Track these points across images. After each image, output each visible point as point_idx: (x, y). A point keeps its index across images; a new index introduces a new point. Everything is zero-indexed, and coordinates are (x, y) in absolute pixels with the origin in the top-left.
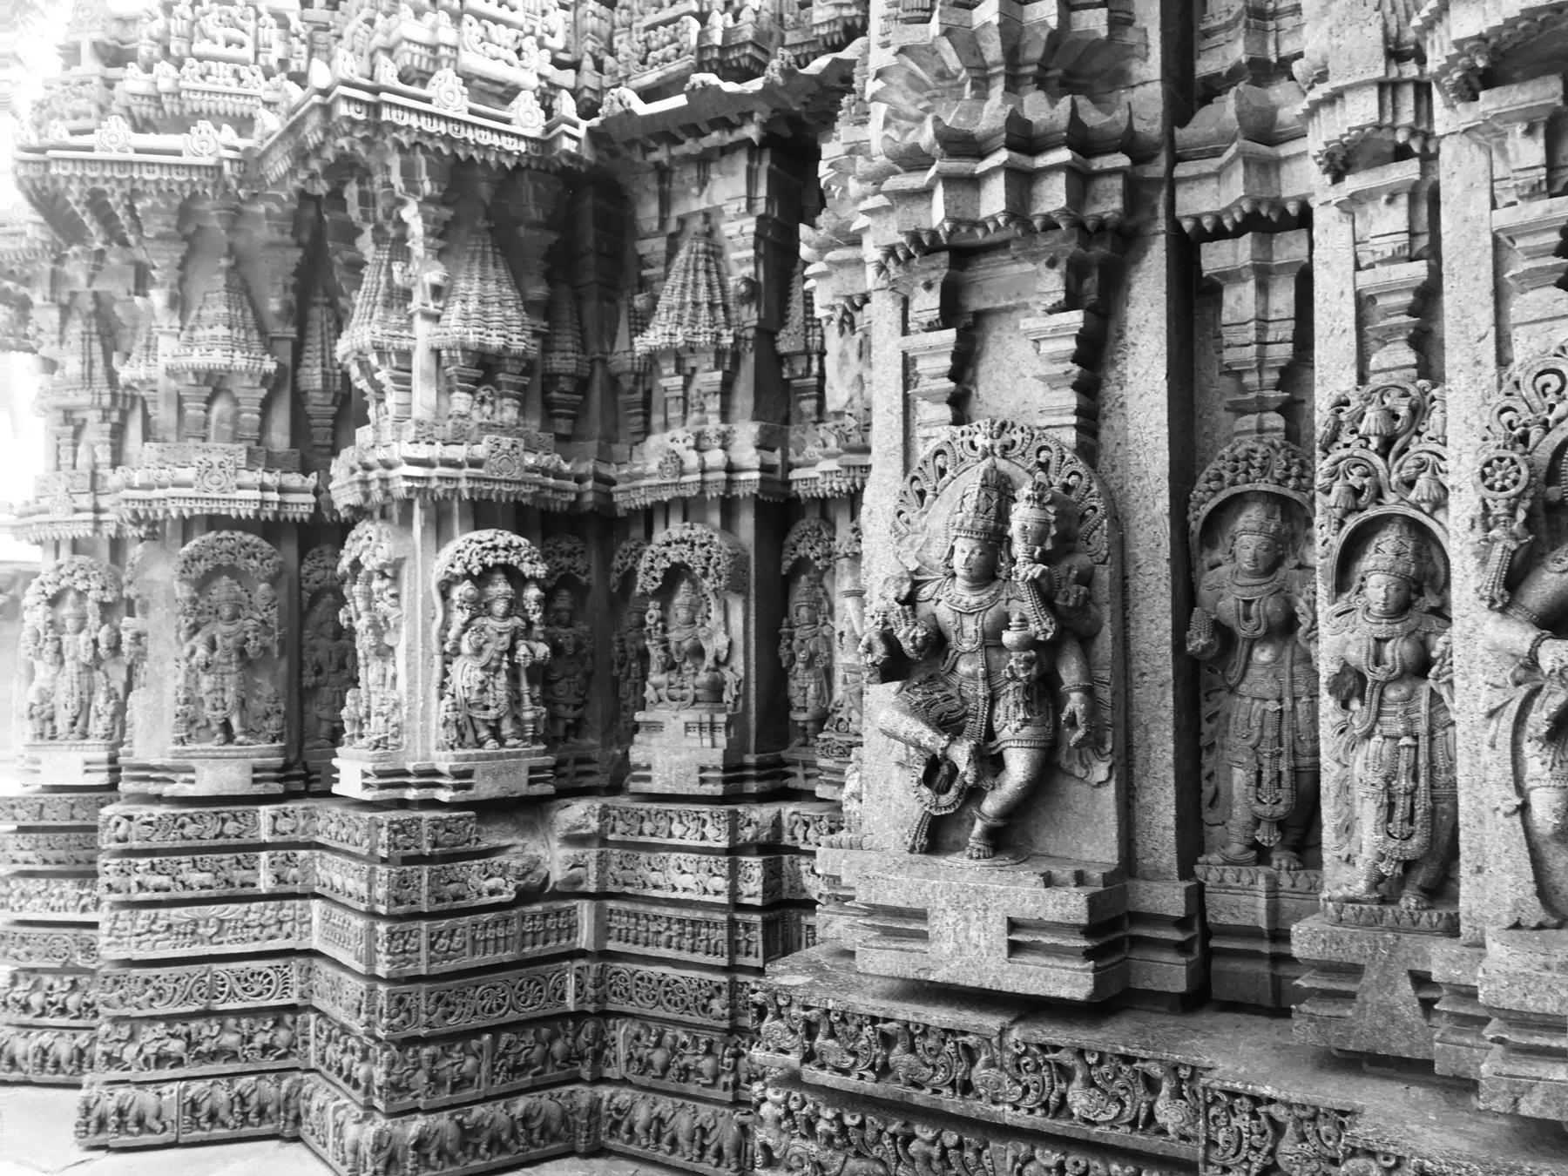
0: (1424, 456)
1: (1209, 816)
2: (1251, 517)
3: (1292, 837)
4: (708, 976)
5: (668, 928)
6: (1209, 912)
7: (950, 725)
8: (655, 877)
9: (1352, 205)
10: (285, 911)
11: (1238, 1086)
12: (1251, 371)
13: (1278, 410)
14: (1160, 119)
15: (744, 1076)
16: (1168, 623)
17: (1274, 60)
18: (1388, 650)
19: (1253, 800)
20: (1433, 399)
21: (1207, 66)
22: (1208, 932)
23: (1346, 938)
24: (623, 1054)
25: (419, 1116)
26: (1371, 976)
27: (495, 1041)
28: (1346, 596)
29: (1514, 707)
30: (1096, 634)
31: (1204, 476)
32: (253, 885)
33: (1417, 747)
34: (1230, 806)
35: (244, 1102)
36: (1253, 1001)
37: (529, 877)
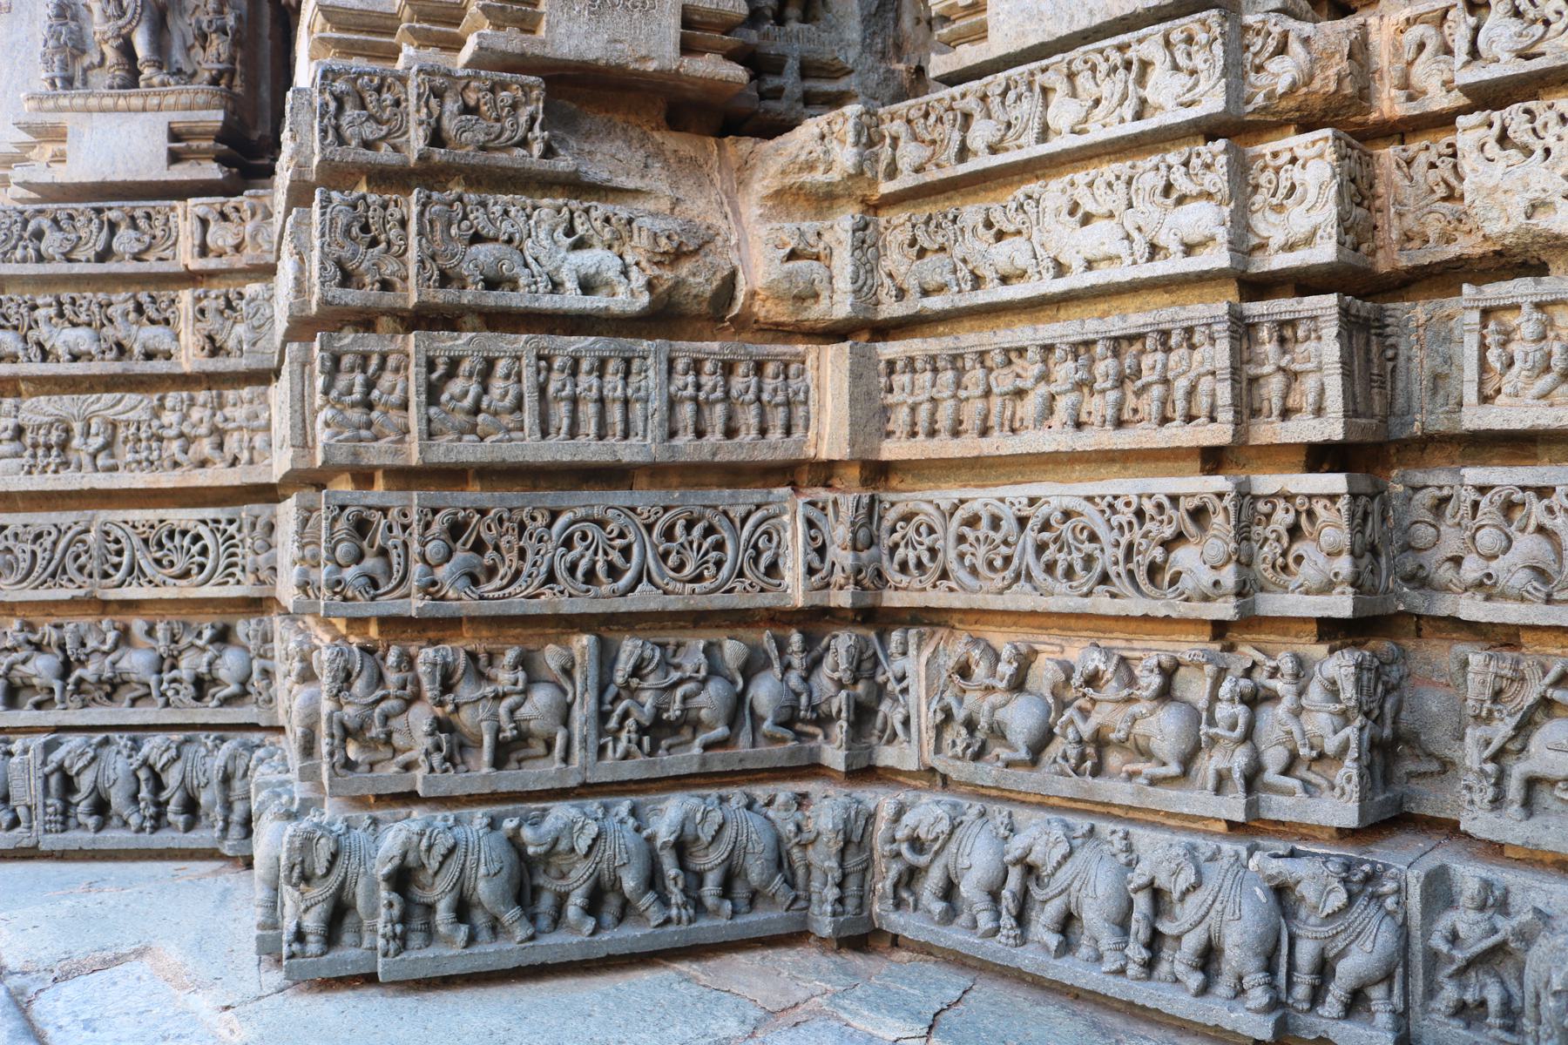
4: (1162, 485)
5: (1044, 377)
8: (1006, 254)
10: (228, 411)
15: (1274, 758)
24: (926, 718)
25: (418, 814)
27: (606, 658)
32: (168, 356)
35: (158, 784)
37: (685, 269)
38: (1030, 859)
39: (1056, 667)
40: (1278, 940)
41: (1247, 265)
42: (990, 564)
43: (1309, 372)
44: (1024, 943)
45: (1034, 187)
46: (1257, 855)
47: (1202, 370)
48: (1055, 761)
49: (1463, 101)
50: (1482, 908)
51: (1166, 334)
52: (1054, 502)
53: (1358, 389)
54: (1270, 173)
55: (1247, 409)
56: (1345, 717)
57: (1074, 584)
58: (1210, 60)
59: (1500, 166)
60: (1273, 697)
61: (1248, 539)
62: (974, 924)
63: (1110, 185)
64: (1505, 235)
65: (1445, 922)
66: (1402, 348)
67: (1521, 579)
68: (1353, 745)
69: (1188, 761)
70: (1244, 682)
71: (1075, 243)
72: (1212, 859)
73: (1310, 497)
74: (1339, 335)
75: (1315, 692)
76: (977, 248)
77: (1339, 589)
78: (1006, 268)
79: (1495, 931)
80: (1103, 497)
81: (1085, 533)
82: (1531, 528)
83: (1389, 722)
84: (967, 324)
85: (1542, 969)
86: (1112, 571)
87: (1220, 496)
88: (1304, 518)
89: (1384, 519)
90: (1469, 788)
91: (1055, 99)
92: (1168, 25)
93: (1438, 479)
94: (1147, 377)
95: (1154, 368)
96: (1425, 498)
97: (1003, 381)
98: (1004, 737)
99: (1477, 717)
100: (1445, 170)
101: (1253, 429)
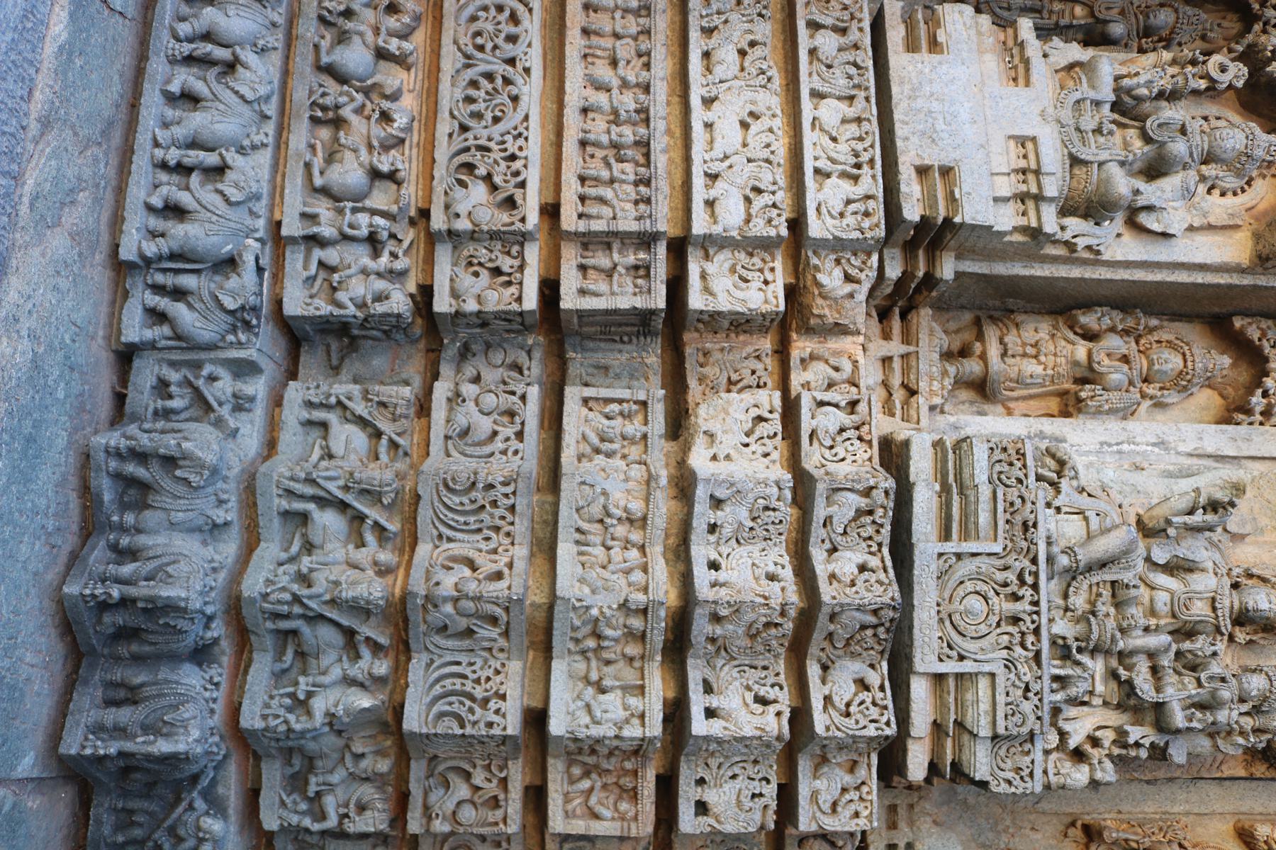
4: (533, 177)
5: (625, 84)
8: (727, 57)
15: (331, 255)
38: (240, 69)
39: (395, 88)
40: (195, 262)
41: (695, 245)
42: (478, 34)
43: (611, 285)
44: (170, 62)
45: (777, 82)
46: (257, 245)
47: (617, 210)
48: (321, 86)
49: (793, 394)
50: (235, 396)
51: (648, 183)
52: (525, 89)
53: (598, 318)
54: (759, 264)
55: (587, 241)
56: (362, 305)
57: (460, 104)
58: (847, 228)
59: (742, 417)
60: (376, 254)
61: (491, 238)
62: (183, 19)
63: (768, 146)
64: (696, 417)
65: (221, 371)
66: (628, 347)
67: (461, 420)
68: (342, 312)
69: (325, 191)
70: (385, 234)
71: (727, 116)
72: (251, 212)
73: (521, 283)
74: (635, 308)
75: (380, 285)
76: (737, 31)
77: (453, 302)
78: (715, 57)
79: (220, 404)
80: (527, 129)
81: (500, 114)
82: (497, 428)
83: (363, 333)
84: (677, 19)
85: (197, 435)
86: (470, 135)
87: (523, 220)
88: (506, 278)
89: (508, 331)
90: (318, 387)
91: (843, 107)
92: (881, 199)
93: (535, 368)
94: (617, 167)
95: (623, 173)
96: (522, 358)
97: (625, 49)
98: (339, 42)
99: (367, 392)
100: (751, 380)
101: (572, 245)
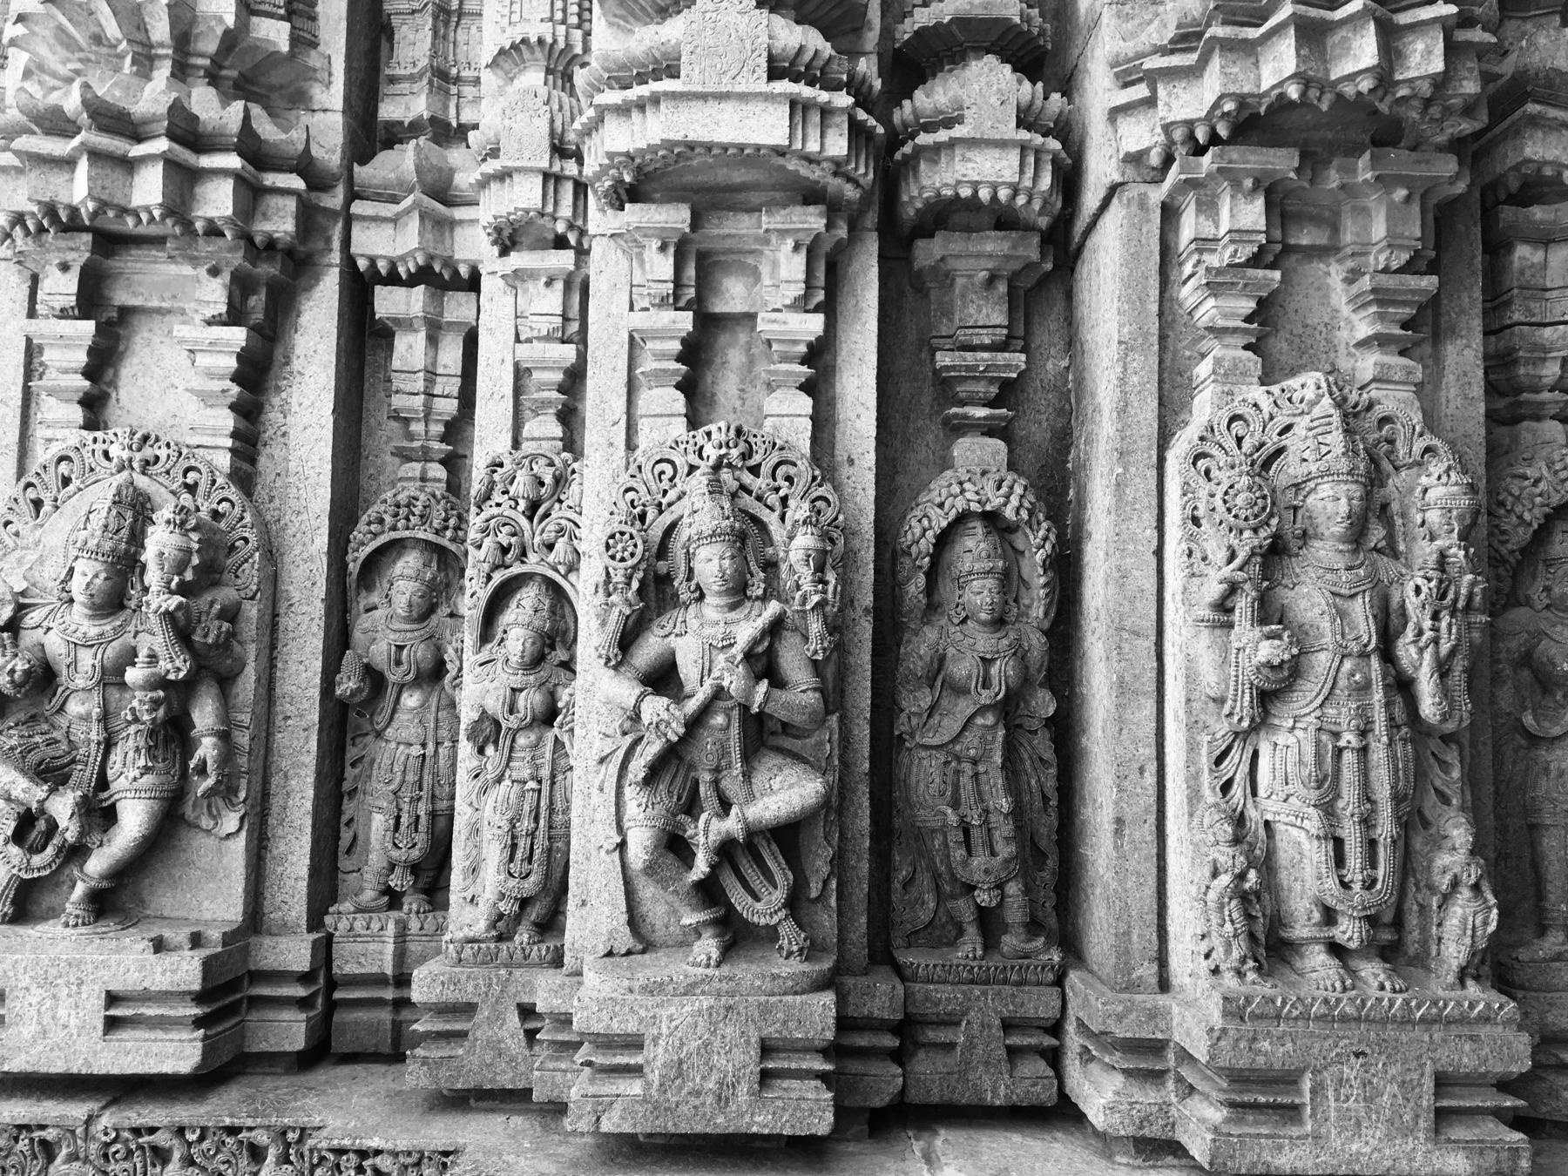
0: (563, 522)
1: (344, 863)
2: (408, 564)
3: (425, 879)
6: (335, 964)
7: (52, 774)
9: (516, 279)
11: (346, 1142)
12: (418, 420)
13: (442, 462)
14: (339, 150)
16: (318, 665)
17: (454, 124)
18: (521, 700)
19: (390, 846)
20: (573, 472)
21: (389, 111)
22: (332, 984)
23: (464, 978)
26: (484, 1013)
28: (489, 646)
29: (620, 754)
30: (238, 675)
31: (365, 518)
33: (540, 791)
34: (367, 852)
36: (372, 1050)
